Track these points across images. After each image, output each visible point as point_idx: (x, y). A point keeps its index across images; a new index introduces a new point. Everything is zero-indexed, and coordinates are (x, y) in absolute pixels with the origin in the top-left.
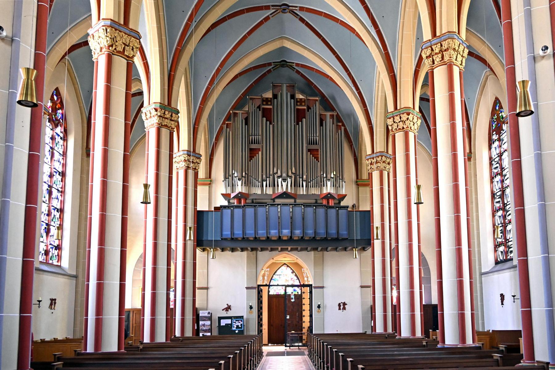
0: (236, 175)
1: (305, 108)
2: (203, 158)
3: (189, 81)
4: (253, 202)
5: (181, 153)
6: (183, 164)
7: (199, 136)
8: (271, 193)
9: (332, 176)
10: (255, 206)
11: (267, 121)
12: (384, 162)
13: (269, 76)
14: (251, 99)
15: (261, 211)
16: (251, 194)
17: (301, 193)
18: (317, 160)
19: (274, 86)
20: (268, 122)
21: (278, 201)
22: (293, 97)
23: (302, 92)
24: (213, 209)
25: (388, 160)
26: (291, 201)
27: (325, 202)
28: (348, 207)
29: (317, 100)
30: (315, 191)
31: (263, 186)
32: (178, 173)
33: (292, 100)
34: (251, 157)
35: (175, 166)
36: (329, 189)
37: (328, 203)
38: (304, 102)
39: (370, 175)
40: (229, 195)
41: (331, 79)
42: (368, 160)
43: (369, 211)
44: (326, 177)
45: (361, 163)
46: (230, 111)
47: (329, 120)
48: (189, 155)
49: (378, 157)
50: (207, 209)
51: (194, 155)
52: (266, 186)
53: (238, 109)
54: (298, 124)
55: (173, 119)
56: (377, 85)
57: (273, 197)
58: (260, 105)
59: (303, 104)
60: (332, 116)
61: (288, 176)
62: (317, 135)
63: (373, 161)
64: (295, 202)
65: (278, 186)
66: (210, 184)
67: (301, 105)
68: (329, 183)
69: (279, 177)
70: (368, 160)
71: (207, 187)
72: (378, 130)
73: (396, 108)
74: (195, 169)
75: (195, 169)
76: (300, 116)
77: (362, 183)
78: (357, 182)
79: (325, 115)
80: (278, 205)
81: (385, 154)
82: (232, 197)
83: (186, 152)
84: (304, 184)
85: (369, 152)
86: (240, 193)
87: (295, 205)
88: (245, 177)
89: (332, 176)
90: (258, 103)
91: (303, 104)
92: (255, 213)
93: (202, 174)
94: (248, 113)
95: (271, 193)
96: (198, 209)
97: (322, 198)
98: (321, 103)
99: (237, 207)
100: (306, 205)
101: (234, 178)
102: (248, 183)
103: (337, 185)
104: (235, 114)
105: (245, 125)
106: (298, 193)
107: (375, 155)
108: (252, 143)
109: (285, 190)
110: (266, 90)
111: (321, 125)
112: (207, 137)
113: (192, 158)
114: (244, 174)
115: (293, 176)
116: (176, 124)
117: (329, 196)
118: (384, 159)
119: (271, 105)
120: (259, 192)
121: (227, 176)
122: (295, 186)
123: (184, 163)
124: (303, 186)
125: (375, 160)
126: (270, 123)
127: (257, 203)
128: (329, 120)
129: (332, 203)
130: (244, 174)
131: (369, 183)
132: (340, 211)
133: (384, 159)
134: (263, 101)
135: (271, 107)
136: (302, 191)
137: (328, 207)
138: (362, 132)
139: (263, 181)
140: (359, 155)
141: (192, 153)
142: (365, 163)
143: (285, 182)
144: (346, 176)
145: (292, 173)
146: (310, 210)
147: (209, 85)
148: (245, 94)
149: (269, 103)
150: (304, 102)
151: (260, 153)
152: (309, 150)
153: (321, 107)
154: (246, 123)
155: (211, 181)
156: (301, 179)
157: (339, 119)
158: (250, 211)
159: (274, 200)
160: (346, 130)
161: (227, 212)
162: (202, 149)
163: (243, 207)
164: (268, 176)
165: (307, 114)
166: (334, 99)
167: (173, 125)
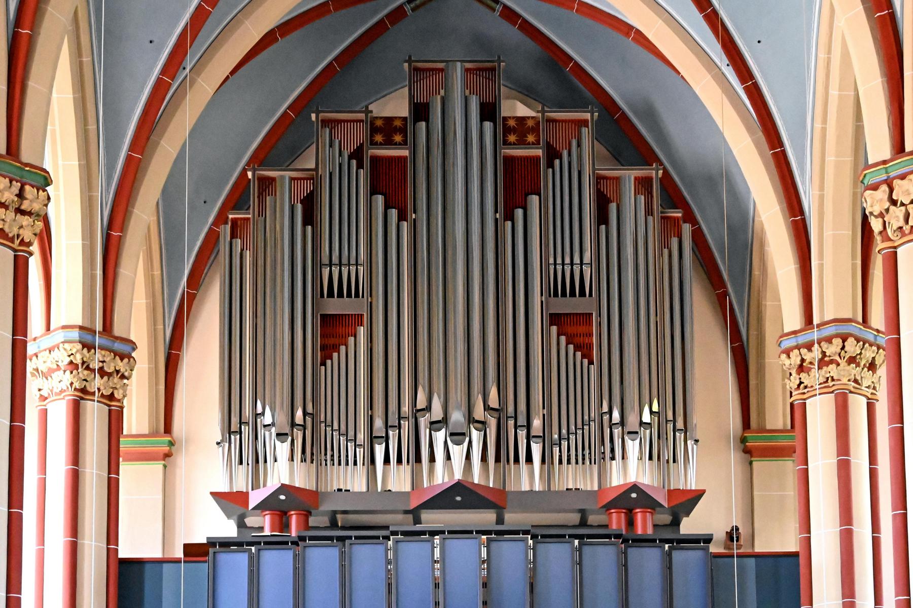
0: (268, 419)
1: (539, 152)
2: (141, 355)
3: (86, 59)
4: (334, 525)
5: (58, 337)
6: (64, 381)
7: (124, 271)
8: (408, 488)
9: (646, 418)
10: (342, 539)
11: (387, 207)
12: (852, 360)
14: (325, 123)
15: (368, 558)
16: (326, 494)
17: (525, 487)
18: (587, 355)
19: (418, 73)
20: (394, 213)
21: (432, 519)
22: (489, 111)
23: (527, 93)
24: (179, 554)
25: (869, 353)
26: (486, 518)
27: (617, 522)
28: (708, 540)
29: (584, 123)
30: (577, 478)
32: (44, 414)
33: (488, 125)
34: (327, 350)
35: (33, 386)
36: (632, 469)
37: (631, 523)
38: (535, 130)
39: (798, 413)
40: (242, 497)
41: (641, 39)
42: (788, 352)
43: (795, 555)
44: (622, 423)
45: (761, 368)
46: (244, 171)
48: (88, 346)
49: (829, 340)
50: (158, 554)
51: (106, 342)
52: (387, 460)
55: (25, 206)
56: (822, 55)
57: (413, 504)
59: (531, 138)
60: (644, 184)
61: (471, 420)
62: (587, 259)
63: (808, 356)
64: (500, 520)
65: (432, 459)
66: (167, 455)
67: (522, 142)
68: (633, 447)
69: (435, 425)
70: (788, 352)
71: (158, 467)
72: (828, 233)
73: (899, 147)
74: (111, 397)
75: (111, 397)
76: (517, 185)
77: (764, 443)
78: (743, 440)
79: (617, 179)
80: (433, 533)
81: (856, 329)
82: (252, 505)
83: (75, 334)
84: (536, 449)
85: (792, 319)
86: (283, 488)
87: (499, 533)
88: (304, 427)
89: (646, 418)
90: (357, 136)
92: (342, 567)
93: (137, 417)
94: (313, 177)
95: (408, 488)
96: (122, 554)
97: (608, 507)
99: (271, 543)
100: (543, 535)
101: (261, 431)
102: (314, 450)
103: (667, 454)
104: (266, 184)
105: (305, 224)
106: (511, 487)
107: (815, 335)
108: (331, 294)
109: (458, 476)
111: (602, 218)
112: (157, 273)
113: (99, 355)
114: (299, 413)
115: (492, 422)
116: (40, 225)
117: (632, 500)
118: (852, 347)
119: (405, 142)
121: (235, 424)
122: (498, 459)
123: (68, 378)
124: (529, 459)
125: (816, 353)
126: (402, 217)
127: (349, 528)
129: (644, 524)
130: (299, 413)
131: (790, 446)
132: (678, 556)
133: (852, 347)
134: (374, 130)
135: (405, 153)
136: (528, 478)
137: (630, 540)
138: (762, 245)
139: (373, 439)
140: (753, 332)
141: (101, 335)
142: (777, 366)
144: (699, 418)
145: (487, 408)
146: (557, 556)
147: (164, 71)
148: (301, 105)
149: (398, 138)
150: (535, 130)
151: (362, 331)
152: (555, 319)
154: (309, 218)
155: (171, 444)
156: (522, 434)
157: (672, 195)
158: (322, 560)
159: (415, 515)
160: (698, 238)
161: (235, 565)
162: (137, 321)
163: (295, 543)
164: (393, 420)
165: (547, 178)
166: (650, 114)
167: (27, 228)
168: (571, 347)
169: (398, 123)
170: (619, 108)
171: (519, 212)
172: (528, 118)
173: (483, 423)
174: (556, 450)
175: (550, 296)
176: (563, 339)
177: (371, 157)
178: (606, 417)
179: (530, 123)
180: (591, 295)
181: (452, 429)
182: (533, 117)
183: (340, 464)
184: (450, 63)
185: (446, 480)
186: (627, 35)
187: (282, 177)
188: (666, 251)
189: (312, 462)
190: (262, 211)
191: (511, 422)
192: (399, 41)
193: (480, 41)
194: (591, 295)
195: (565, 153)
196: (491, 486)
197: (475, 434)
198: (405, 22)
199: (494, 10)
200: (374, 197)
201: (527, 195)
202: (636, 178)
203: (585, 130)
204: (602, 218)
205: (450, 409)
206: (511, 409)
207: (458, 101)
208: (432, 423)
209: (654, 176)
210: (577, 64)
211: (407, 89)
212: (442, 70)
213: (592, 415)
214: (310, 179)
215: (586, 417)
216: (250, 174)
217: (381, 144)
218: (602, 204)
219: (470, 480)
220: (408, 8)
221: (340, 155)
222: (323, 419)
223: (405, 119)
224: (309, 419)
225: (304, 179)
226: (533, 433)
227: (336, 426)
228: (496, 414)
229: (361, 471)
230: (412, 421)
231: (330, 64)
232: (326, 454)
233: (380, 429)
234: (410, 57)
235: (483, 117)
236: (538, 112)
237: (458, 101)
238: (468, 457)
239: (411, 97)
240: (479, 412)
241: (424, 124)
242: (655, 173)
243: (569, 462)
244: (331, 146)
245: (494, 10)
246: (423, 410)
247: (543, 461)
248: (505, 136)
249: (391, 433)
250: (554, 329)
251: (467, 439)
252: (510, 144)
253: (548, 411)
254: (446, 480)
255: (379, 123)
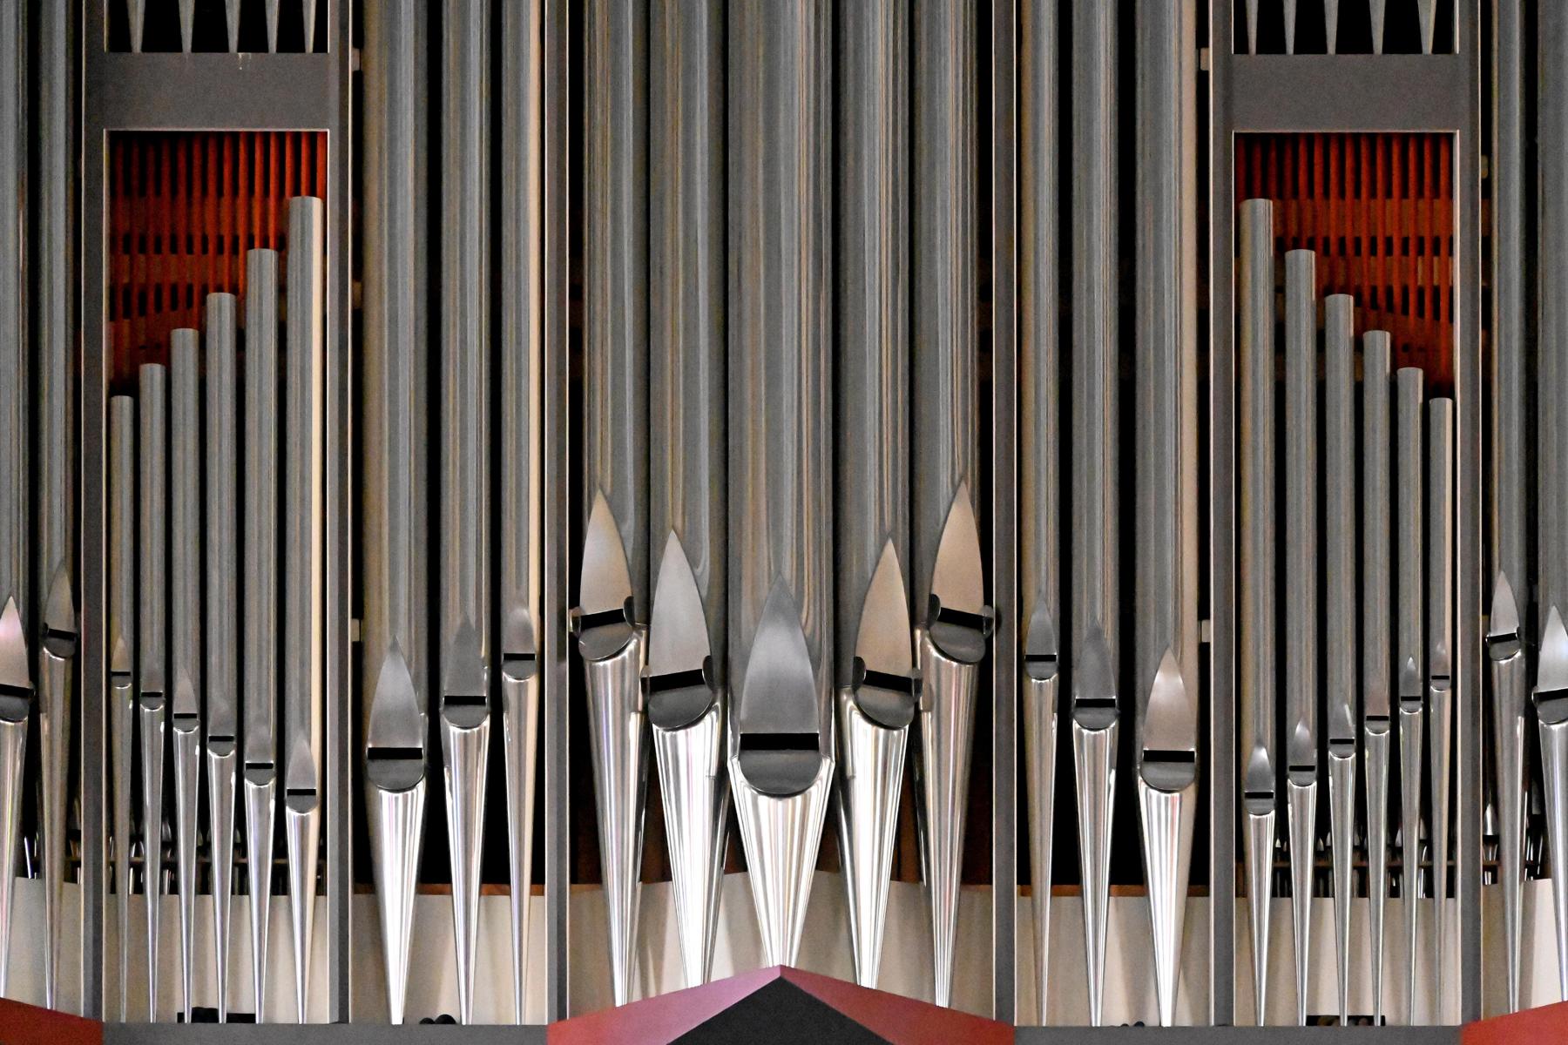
17: (1109, 1007)
18: (1422, 351)
31: (365, 873)
52: (433, 870)
61: (844, 669)
65: (655, 864)
69: (669, 696)
106: (1037, 1008)
109: (780, 948)
115: (952, 685)
120: (289, 973)
122: (975, 870)
124: (1129, 869)
136: (1129, 955)
139: (364, 763)
143: (781, 788)
145: (926, 611)
152: (1265, 163)
156: (1096, 742)
164: (465, 668)
168: (1343, 307)
173: (904, 685)
174: (1262, 823)
175: (1242, 47)
176: (1304, 262)
178: (1509, 663)
180: (1443, 42)
181: (747, 717)
183: (204, 887)
185: (723, 970)
189: (70, 876)
191: (1043, 687)
194: (1443, 42)
196: (942, 1001)
197: (864, 740)
205: (744, 611)
206: (1042, 617)
208: (656, 685)
213: (1442, 649)
215: (1411, 664)
219: (839, 973)
222: (122, 661)
224: (54, 662)
226: (1148, 741)
227: (185, 698)
228: (971, 646)
229: (308, 917)
230: (558, 670)
232: (137, 837)
233: (406, 716)
238: (831, 856)
240: (886, 635)
243: (1323, 886)
246: (611, 618)
247: (1197, 879)
249: (453, 733)
250: (1261, 211)
251: (827, 768)
253: (1222, 629)
254: (723, 970)
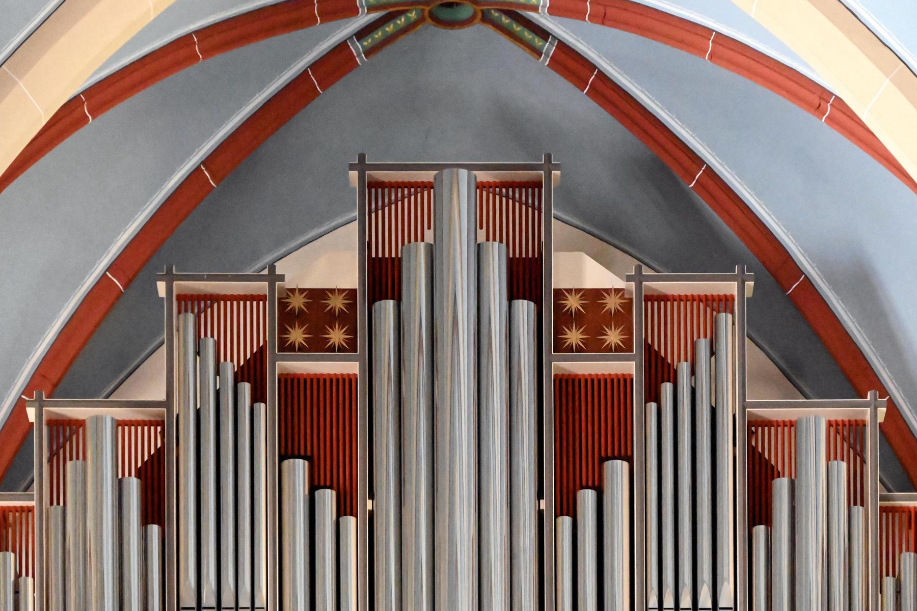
1: (629, 367)
11: (314, 487)
13: (336, 102)
14: (187, 301)
20: (328, 499)
22: (526, 278)
23: (608, 233)
29: (725, 303)
33: (524, 308)
38: (622, 318)
46: (19, 409)
47: (818, 480)
53: (87, 393)
54: (567, 506)
58: (259, 358)
59: (613, 337)
60: (847, 437)
67: (594, 346)
76: (582, 436)
90: (252, 330)
91: (613, 337)
94: (163, 423)
98: (756, 330)
104: (65, 434)
105: (146, 520)
110: (303, 227)
111: (759, 510)
119: (351, 346)
126: (345, 507)
128: (818, 480)
134: (287, 317)
135: (351, 367)
149: (337, 336)
150: (622, 318)
153: (756, 356)
154: (155, 509)
165: (645, 418)
166: (863, 284)
169: (337, 303)
170: (797, 271)
171: (587, 498)
172: (607, 291)
177: (280, 376)
179: (612, 303)
182: (617, 291)
184: (446, 172)
186: (818, 110)
187: (98, 420)
188: (889, 582)
190: (57, 493)
192: (337, 125)
193: (511, 122)
195: (684, 369)
198: (351, 78)
199: (538, 53)
200: (286, 463)
201: (602, 460)
202: (830, 424)
203: (725, 320)
204: (759, 510)
207: (462, 255)
209: (868, 418)
210: (710, 172)
211: (356, 224)
212: (428, 186)
214: (156, 424)
216: (31, 413)
217: (301, 349)
218: (760, 477)
220: (357, 48)
221: (217, 372)
223: (352, 293)
225: (143, 423)
231: (196, 173)
234: (362, 157)
235: (514, 293)
236: (629, 279)
237: (462, 255)
239: (365, 246)
241: (391, 303)
242: (870, 413)
244: (198, 353)
245: (538, 53)
248: (558, 331)
252: (570, 349)
255: (297, 302)
